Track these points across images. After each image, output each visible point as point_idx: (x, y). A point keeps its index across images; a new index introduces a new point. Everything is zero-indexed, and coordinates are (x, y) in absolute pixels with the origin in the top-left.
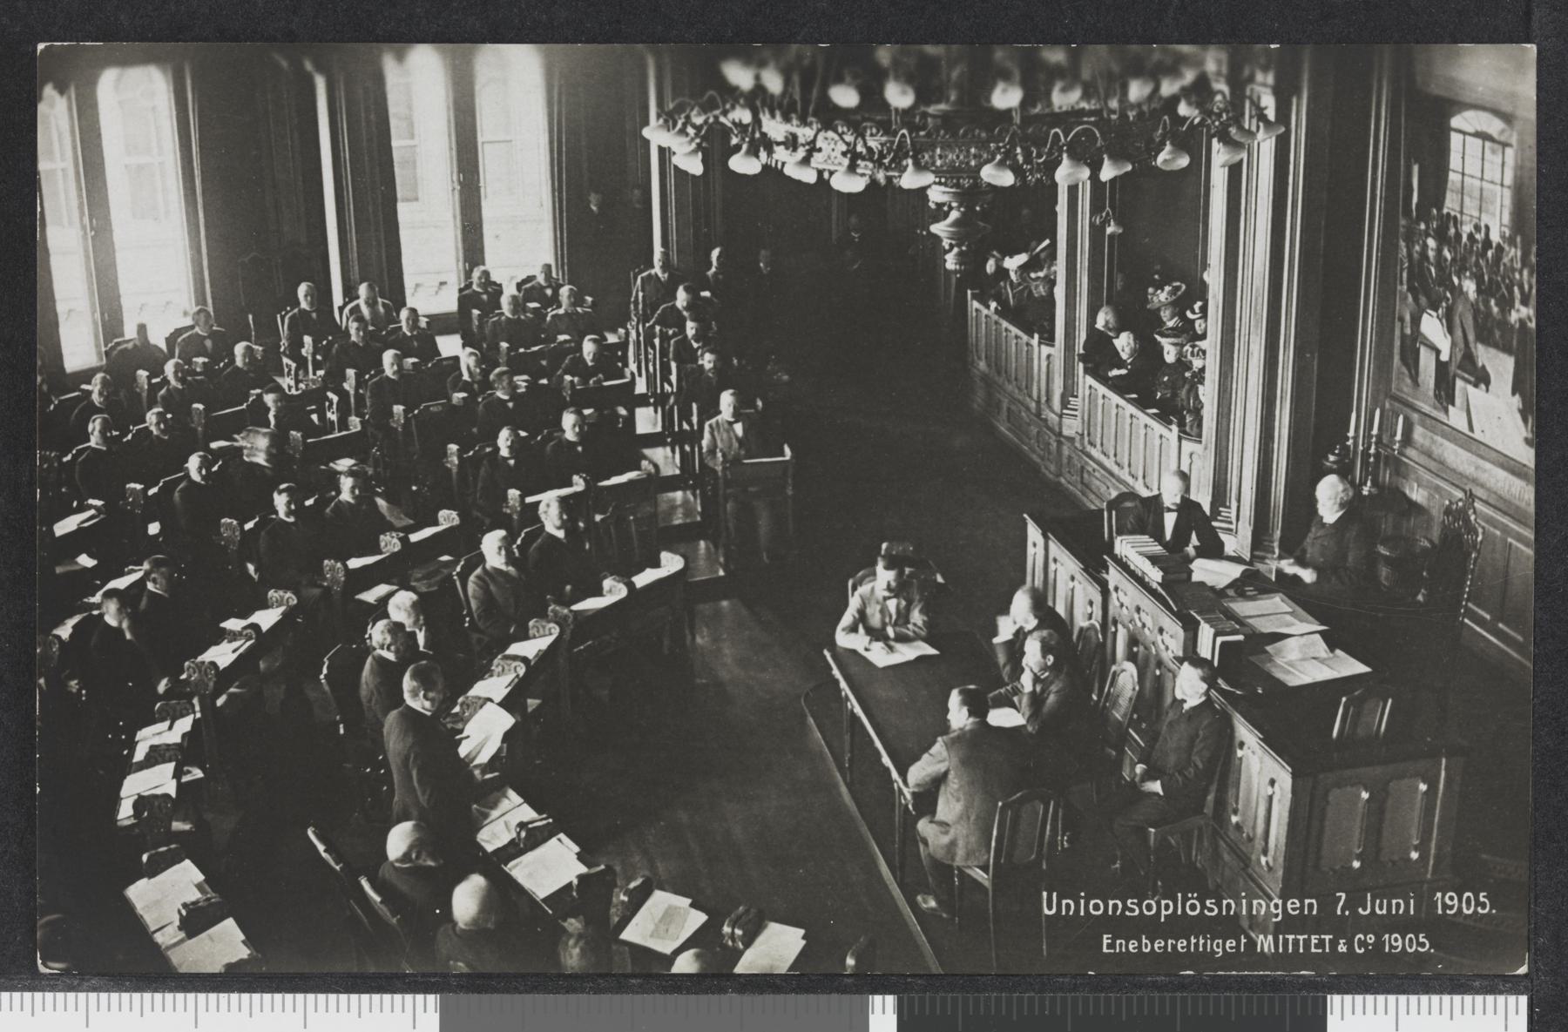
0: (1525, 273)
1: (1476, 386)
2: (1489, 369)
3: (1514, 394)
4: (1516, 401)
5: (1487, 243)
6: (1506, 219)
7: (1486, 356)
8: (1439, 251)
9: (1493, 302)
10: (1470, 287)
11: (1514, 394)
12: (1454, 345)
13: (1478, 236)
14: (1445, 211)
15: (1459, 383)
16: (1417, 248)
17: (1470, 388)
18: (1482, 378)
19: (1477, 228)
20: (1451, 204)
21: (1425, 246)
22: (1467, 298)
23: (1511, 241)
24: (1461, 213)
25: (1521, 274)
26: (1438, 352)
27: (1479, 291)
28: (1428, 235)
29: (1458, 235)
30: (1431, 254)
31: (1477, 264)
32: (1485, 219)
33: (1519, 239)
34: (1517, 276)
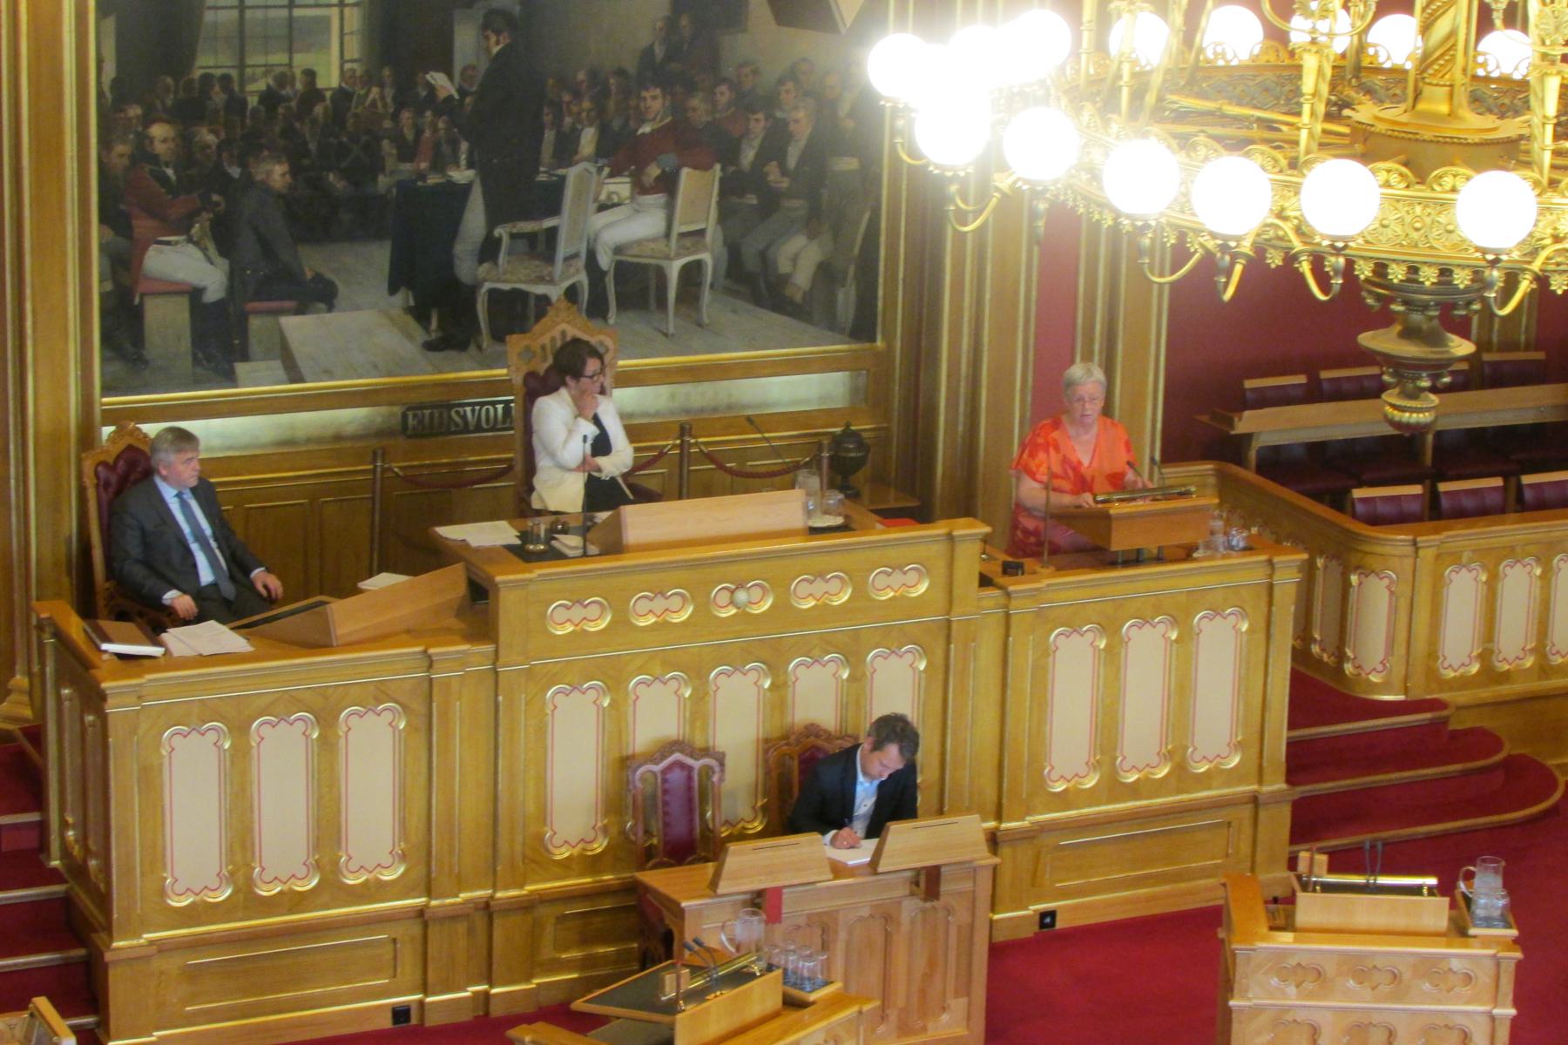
0: (406, 116)
1: (300, 311)
2: (329, 275)
3: (393, 290)
4: (403, 298)
5: (313, 94)
6: (354, 49)
7: (313, 261)
8: (185, 140)
9: (331, 177)
10: (277, 174)
11: (393, 290)
12: (232, 276)
13: (288, 91)
14: (197, 74)
15: (255, 323)
16: (120, 148)
17: (290, 323)
18: (320, 295)
19: (284, 80)
20: (209, 61)
21: (143, 141)
22: (265, 188)
23: (370, 79)
24: (242, 66)
25: (395, 117)
26: (195, 294)
27: (295, 171)
28: (148, 120)
29: (236, 104)
30: (160, 148)
31: (289, 132)
32: (302, 60)
33: (386, 72)
34: (387, 124)
